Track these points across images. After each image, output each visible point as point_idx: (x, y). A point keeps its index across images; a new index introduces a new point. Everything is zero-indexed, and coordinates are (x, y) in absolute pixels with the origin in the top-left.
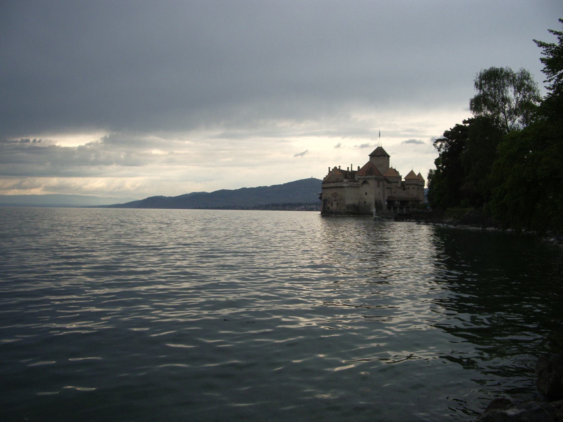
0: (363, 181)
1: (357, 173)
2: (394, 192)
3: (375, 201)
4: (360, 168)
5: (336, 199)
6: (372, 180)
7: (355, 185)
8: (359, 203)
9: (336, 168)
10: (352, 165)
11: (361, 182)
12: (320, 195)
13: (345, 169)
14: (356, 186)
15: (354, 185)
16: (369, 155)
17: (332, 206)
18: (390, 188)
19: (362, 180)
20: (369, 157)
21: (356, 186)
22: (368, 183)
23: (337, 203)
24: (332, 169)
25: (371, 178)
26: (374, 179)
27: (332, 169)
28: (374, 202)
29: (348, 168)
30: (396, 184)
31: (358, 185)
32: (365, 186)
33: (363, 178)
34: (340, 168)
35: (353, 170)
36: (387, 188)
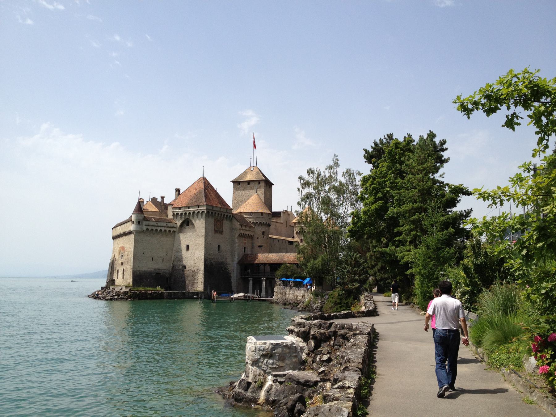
0: (183, 219)
2: (260, 246)
3: (206, 265)
6: (200, 216)
7: (163, 229)
8: (172, 269)
14: (165, 230)
15: (159, 229)
16: (231, 182)
17: (118, 278)
18: (252, 237)
21: (165, 230)
22: (193, 224)
26: (204, 215)
28: (202, 268)
30: (264, 229)
31: (172, 230)
33: (182, 214)
36: (241, 236)
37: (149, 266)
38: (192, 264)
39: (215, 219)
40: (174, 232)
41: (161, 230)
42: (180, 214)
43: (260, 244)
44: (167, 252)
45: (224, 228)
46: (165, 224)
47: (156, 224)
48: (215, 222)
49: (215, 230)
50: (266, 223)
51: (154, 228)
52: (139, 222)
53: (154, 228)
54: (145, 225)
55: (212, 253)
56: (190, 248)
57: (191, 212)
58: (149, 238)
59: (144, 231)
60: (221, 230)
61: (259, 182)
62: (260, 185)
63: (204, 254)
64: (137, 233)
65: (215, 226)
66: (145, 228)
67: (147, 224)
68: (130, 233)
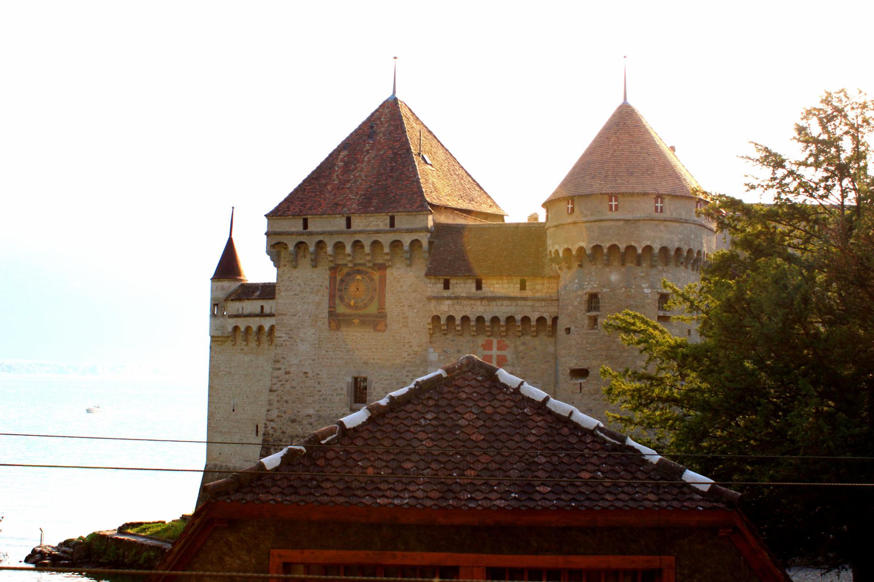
39: (331, 269)
43: (574, 364)
45: (390, 299)
47: (258, 311)
48: (333, 279)
49: (332, 314)
50: (568, 250)
51: (254, 323)
55: (311, 411)
58: (247, 359)
60: (373, 309)
65: (332, 297)
66: (231, 323)
67: (235, 313)
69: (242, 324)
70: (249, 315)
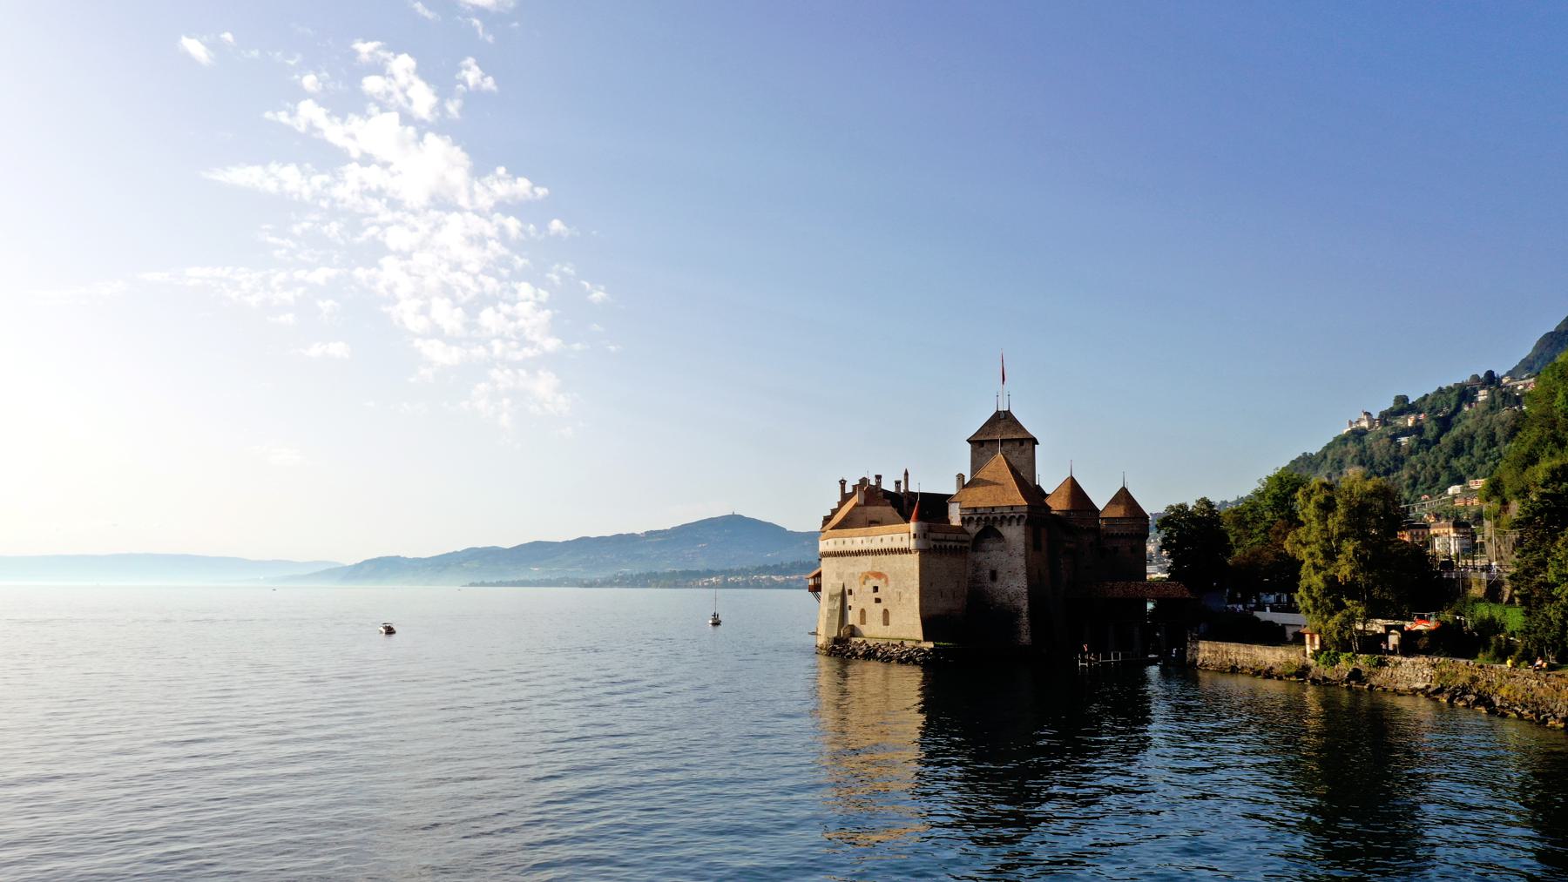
0: (981, 528)
1: (956, 499)
3: (1030, 603)
4: (967, 479)
5: (877, 595)
6: (1014, 523)
7: (953, 544)
9: (864, 481)
10: (906, 474)
11: (973, 529)
12: (814, 577)
13: (892, 489)
15: (948, 544)
17: (863, 622)
19: (978, 525)
20: (969, 445)
21: (956, 546)
22: (1000, 536)
23: (886, 612)
24: (854, 487)
25: (1014, 516)
26: (1022, 523)
27: (854, 487)
28: (1025, 608)
29: (898, 483)
32: (989, 544)
33: (979, 519)
34: (879, 483)
35: (910, 490)
37: (942, 606)
38: (1006, 600)
40: (966, 547)
41: (950, 546)
42: (975, 519)
44: (958, 582)
46: (953, 536)
52: (925, 537)
53: (943, 544)
54: (933, 540)
56: (1000, 576)
57: (999, 517)
59: (930, 549)
61: (1021, 441)
62: (1023, 447)
63: (1026, 586)
64: (924, 553)
66: (932, 544)
68: (906, 551)
69: (938, 544)
70: (952, 541)
